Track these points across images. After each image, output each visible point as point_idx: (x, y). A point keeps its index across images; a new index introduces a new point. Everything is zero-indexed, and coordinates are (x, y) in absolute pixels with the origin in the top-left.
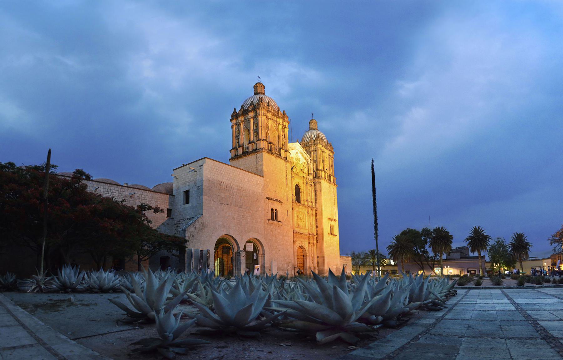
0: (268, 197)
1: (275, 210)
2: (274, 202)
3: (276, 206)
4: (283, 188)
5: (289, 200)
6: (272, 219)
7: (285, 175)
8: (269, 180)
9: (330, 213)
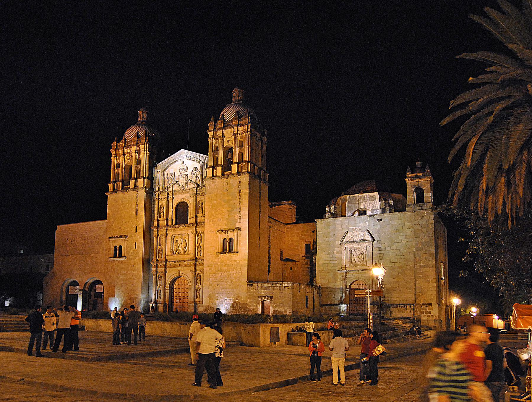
0: (110, 236)
1: (118, 247)
2: (115, 239)
3: (120, 242)
4: (130, 221)
5: (139, 231)
6: (115, 256)
7: (134, 206)
8: (113, 220)
9: (225, 222)
